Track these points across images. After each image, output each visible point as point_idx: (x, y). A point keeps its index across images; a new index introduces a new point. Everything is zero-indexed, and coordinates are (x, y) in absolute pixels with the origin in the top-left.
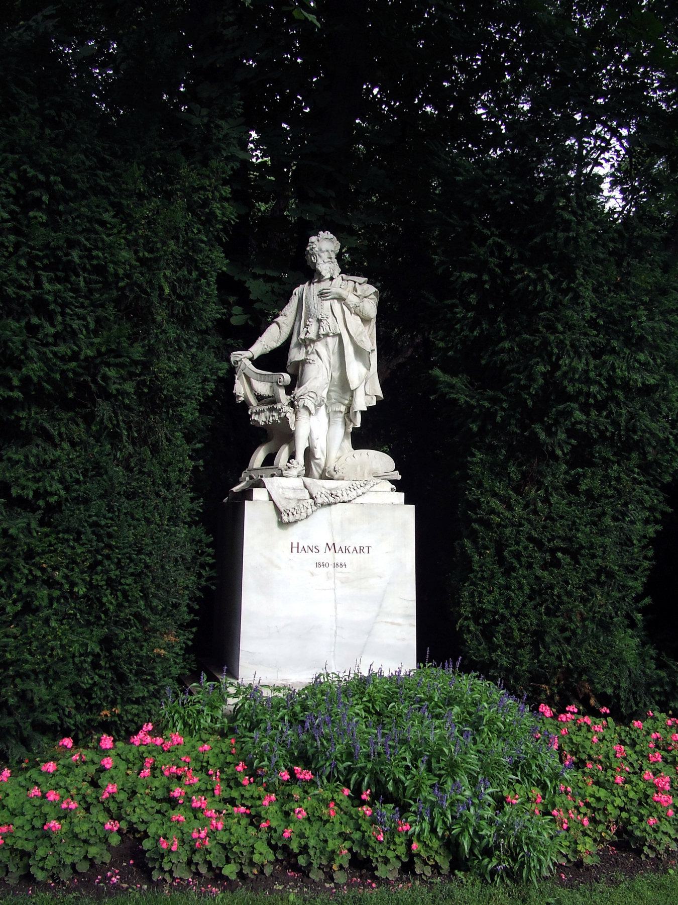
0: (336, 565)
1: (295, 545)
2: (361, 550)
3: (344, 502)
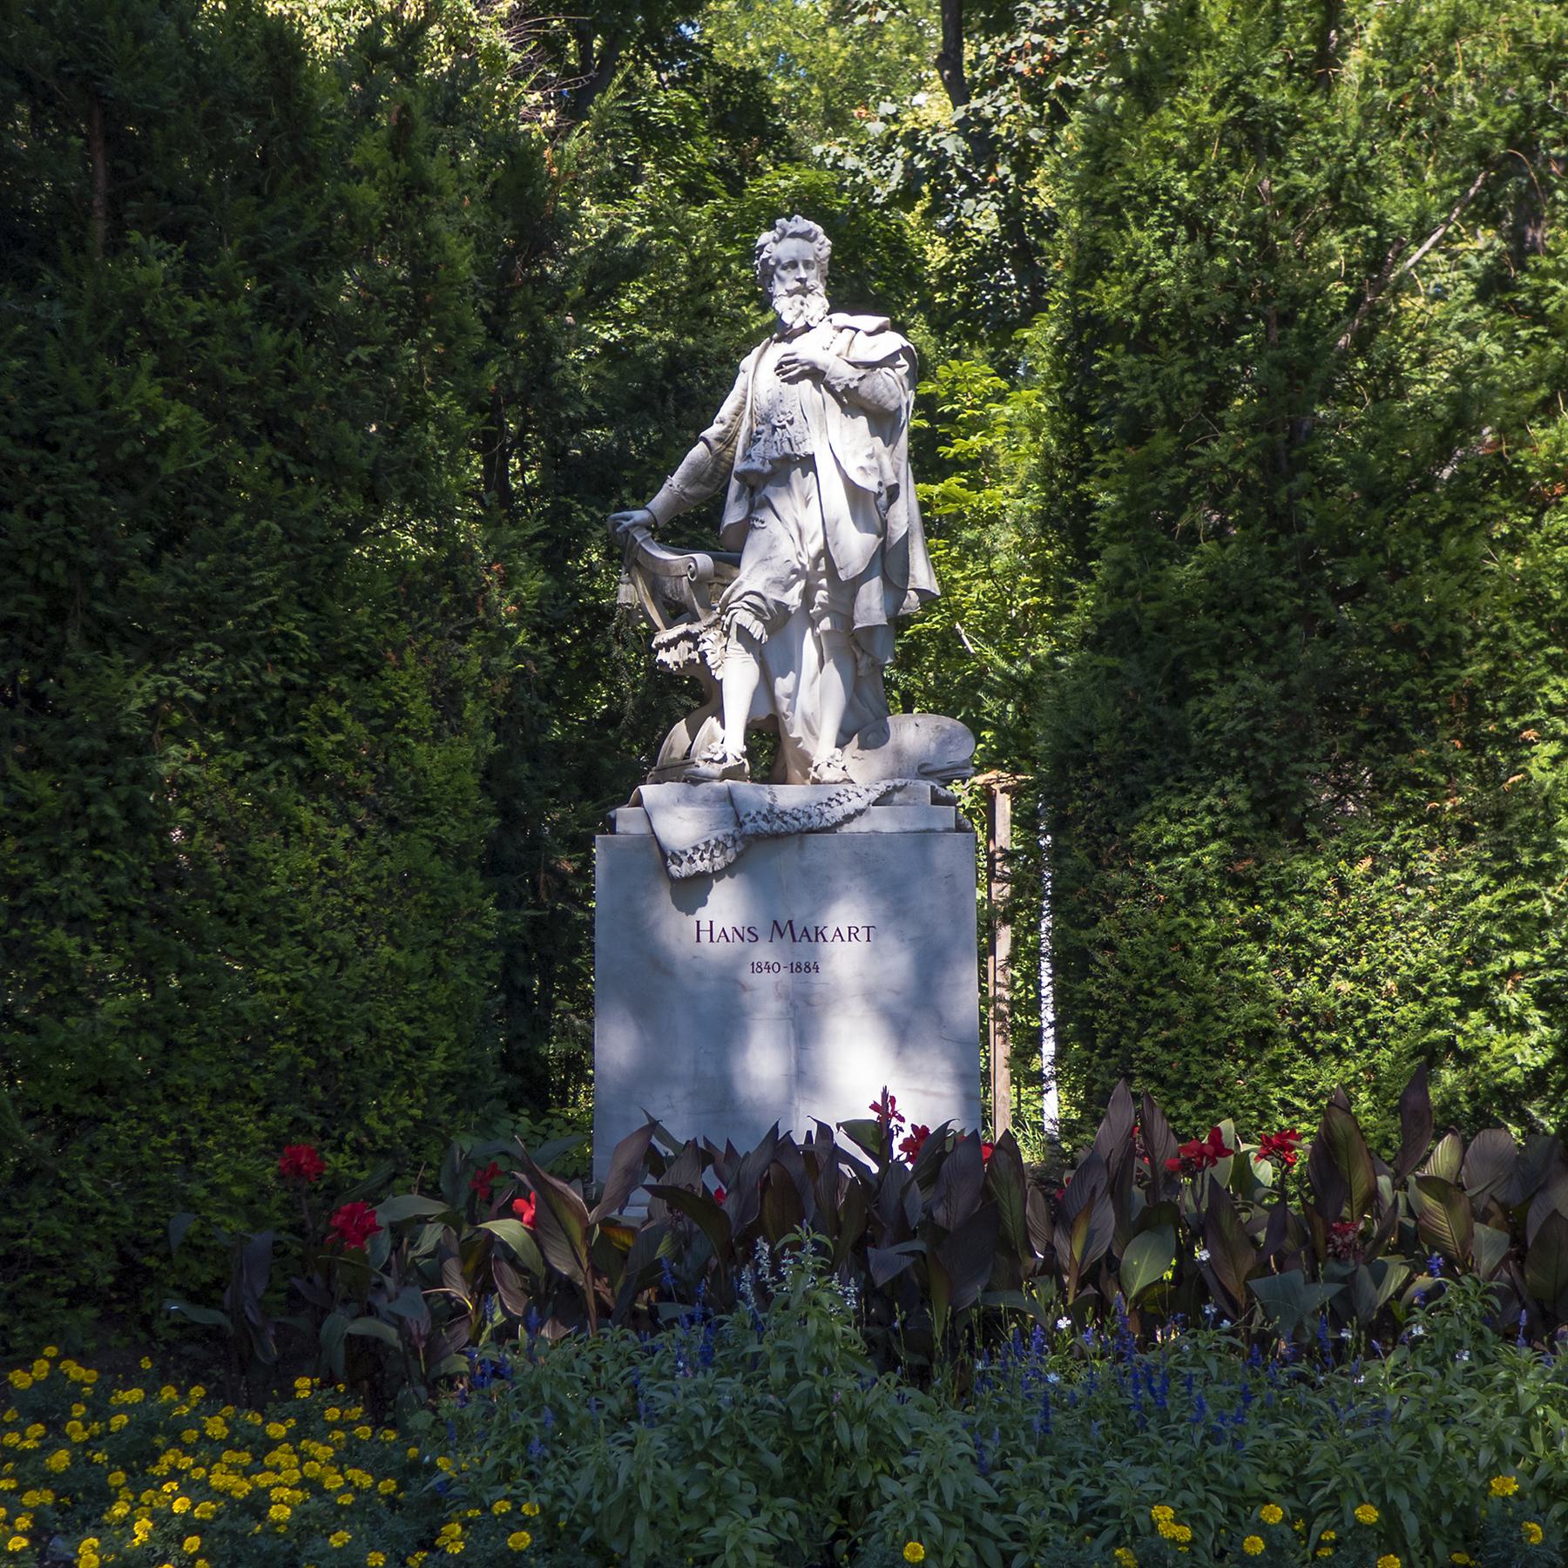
1: (705, 926)
3: (811, 831)
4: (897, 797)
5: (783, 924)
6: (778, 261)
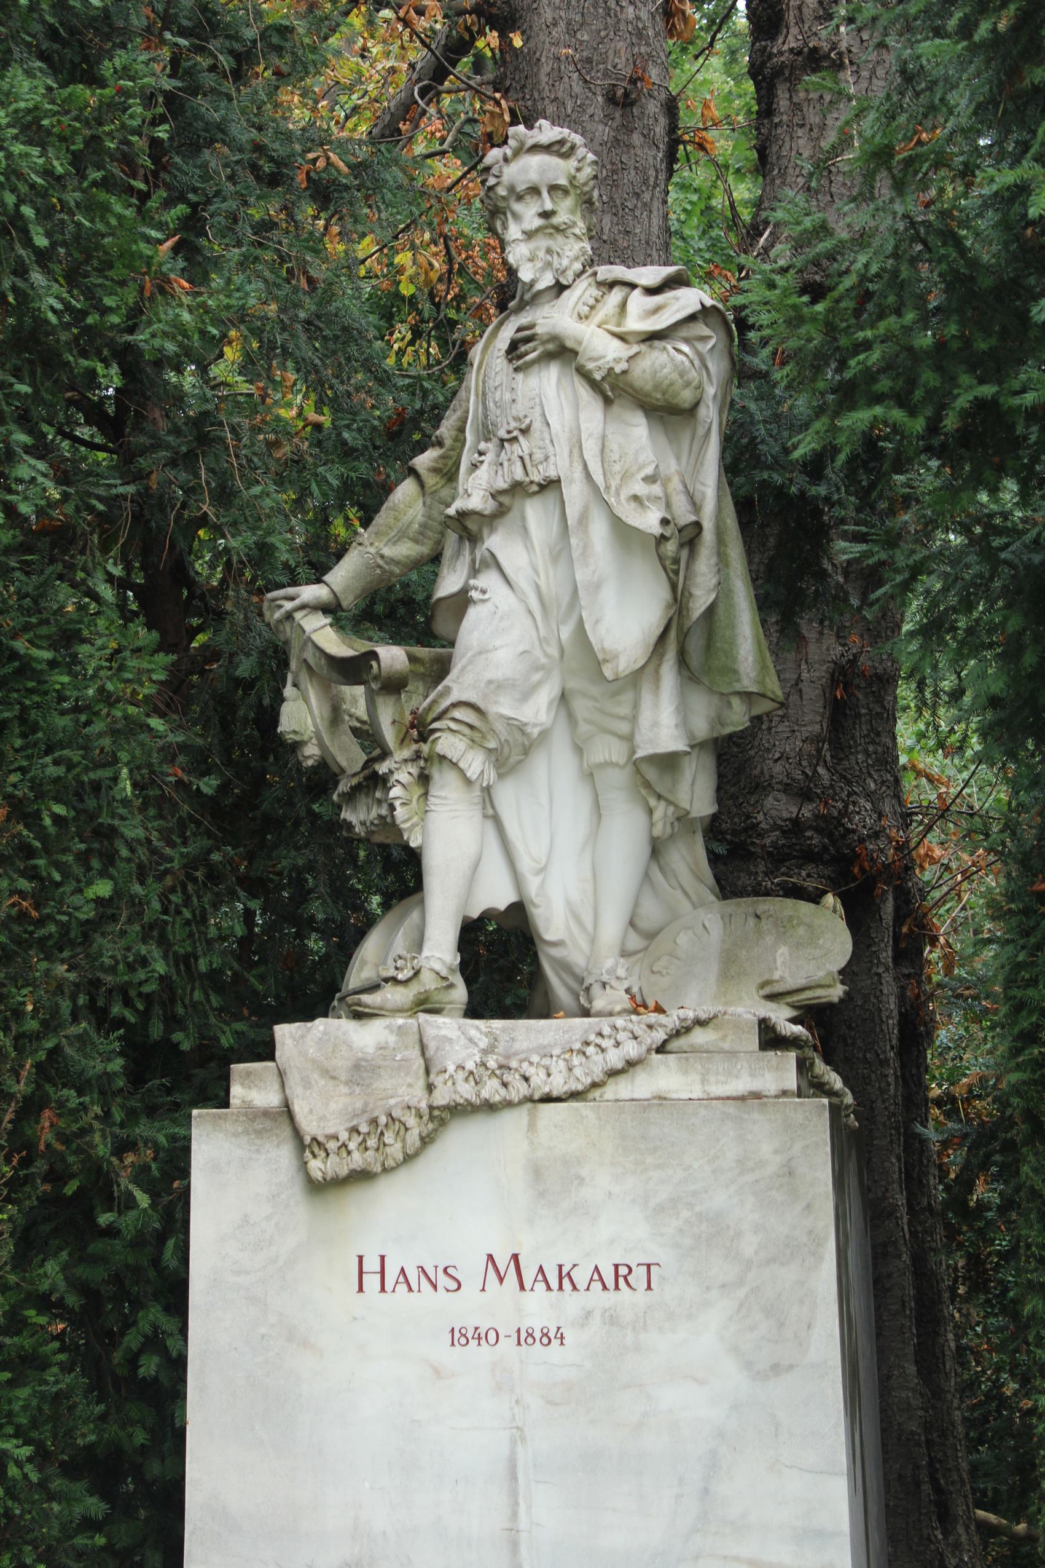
0: (524, 1337)
1: (372, 1264)
2: (622, 1276)
3: (548, 1099)
4: (699, 1037)
5: (502, 1261)
6: (512, 189)
